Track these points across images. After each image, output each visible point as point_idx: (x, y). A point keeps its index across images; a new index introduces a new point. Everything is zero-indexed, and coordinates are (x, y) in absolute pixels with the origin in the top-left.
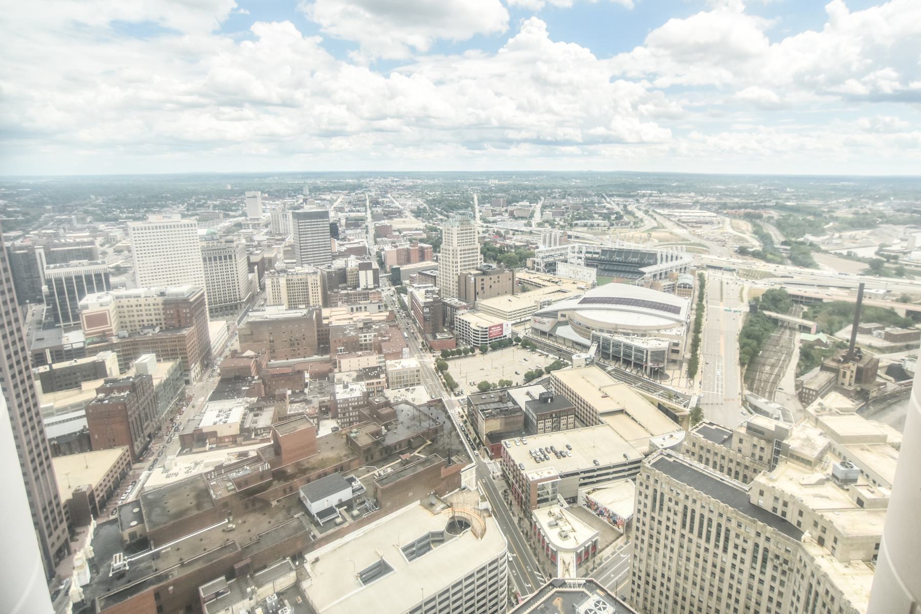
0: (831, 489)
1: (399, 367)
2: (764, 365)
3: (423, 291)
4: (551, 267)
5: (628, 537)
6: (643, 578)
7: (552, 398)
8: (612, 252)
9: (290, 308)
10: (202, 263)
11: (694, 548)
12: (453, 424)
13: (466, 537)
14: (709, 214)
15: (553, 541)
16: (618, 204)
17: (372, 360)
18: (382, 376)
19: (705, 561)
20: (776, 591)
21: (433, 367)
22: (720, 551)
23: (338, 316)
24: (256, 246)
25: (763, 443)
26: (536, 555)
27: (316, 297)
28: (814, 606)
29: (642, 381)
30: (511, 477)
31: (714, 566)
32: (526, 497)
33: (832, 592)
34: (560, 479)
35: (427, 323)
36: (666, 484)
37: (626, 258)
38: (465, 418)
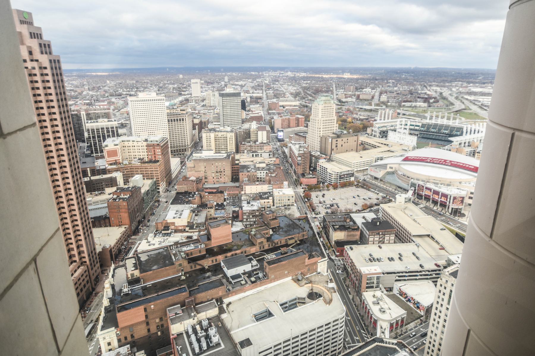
1: (281, 193)
3: (297, 146)
4: (384, 134)
7: (380, 222)
8: (429, 126)
9: (216, 153)
10: (167, 122)
12: (314, 232)
16: (436, 92)
17: (264, 188)
18: (271, 198)
21: (302, 195)
23: (244, 159)
24: (197, 114)
26: (363, 321)
27: (232, 147)
29: (445, 216)
30: (349, 270)
32: (359, 284)
34: (382, 275)
37: (440, 130)
38: (321, 229)
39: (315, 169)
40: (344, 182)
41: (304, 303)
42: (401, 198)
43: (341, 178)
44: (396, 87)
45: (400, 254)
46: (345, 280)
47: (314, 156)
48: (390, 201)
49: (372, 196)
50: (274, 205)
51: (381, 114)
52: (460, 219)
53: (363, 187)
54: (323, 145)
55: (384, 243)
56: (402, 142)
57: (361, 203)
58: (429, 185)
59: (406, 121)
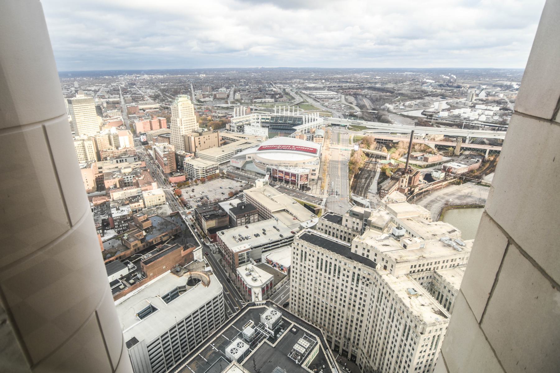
0: (392, 241)
2: (362, 179)
4: (241, 129)
5: (289, 277)
6: (297, 297)
7: (245, 206)
11: (322, 278)
13: (200, 287)
14: (332, 93)
15: (249, 283)
16: (280, 88)
19: (329, 284)
20: (363, 294)
21: (173, 193)
22: (336, 278)
25: (358, 221)
26: (240, 292)
28: (381, 299)
29: (296, 192)
30: (223, 252)
31: (333, 286)
32: (233, 262)
33: (389, 291)
35: (166, 167)
36: (308, 247)
37: (285, 121)
39: (182, 166)
40: (210, 176)
41: (185, 291)
42: (259, 183)
43: (207, 172)
44: (247, 85)
45: (264, 230)
46: (221, 261)
47: (179, 155)
48: (252, 186)
49: (235, 185)
50: (145, 207)
51: (236, 110)
52: (307, 192)
53: (227, 178)
54: (187, 144)
55: (250, 223)
56: (257, 135)
57: (227, 192)
58: (281, 169)
59: (257, 115)
